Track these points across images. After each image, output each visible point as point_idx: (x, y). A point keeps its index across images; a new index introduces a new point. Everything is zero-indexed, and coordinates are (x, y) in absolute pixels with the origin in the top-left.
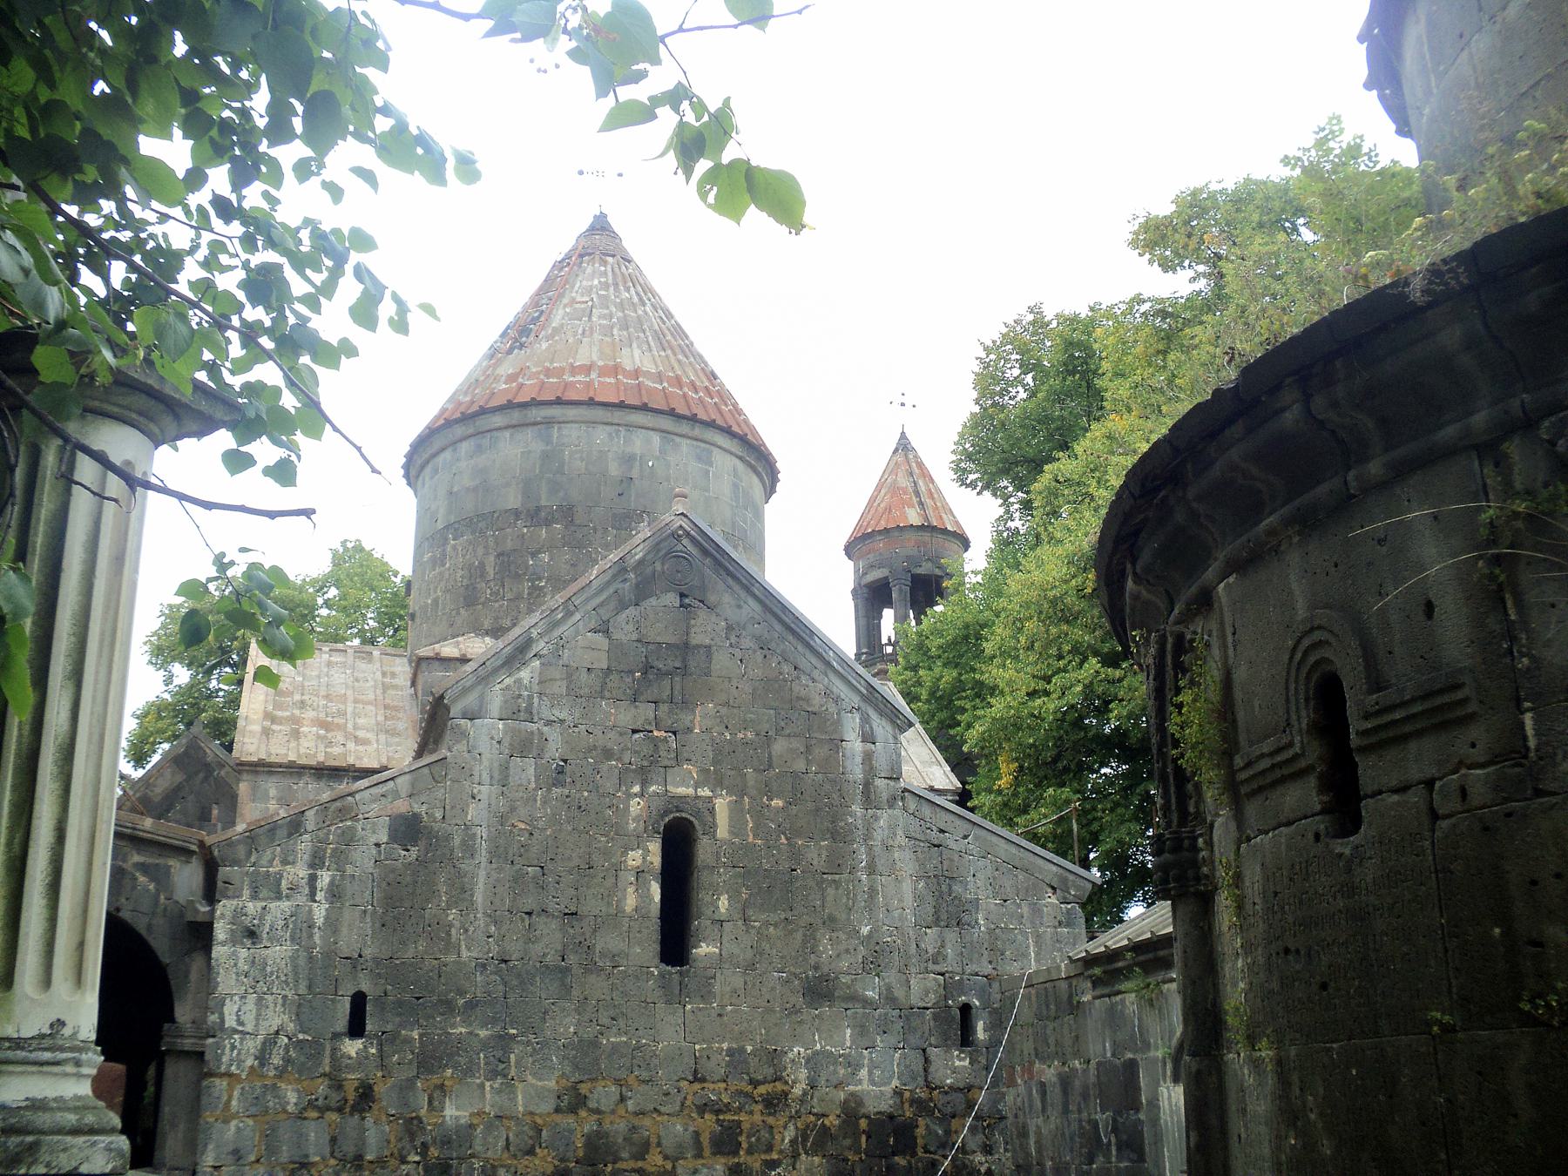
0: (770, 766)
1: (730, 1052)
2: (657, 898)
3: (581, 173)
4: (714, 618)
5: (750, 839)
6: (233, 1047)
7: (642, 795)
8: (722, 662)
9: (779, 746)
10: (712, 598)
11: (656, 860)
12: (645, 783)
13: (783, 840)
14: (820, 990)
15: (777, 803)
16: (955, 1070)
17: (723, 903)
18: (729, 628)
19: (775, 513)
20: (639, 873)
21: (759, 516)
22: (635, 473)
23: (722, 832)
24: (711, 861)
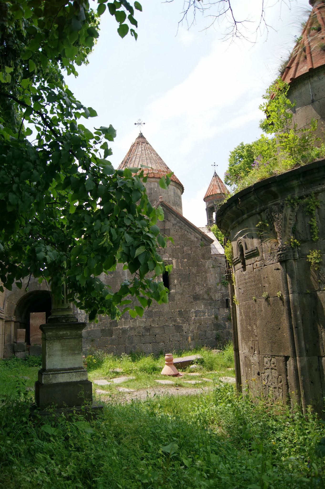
0: (184, 253)
1: (179, 311)
3: (135, 124)
4: (170, 223)
6: (80, 317)
8: (172, 232)
9: (185, 248)
10: (169, 219)
14: (196, 298)
15: (186, 260)
16: (225, 313)
17: (176, 281)
18: (173, 225)
19: (184, 197)
21: (180, 198)
22: (152, 192)
24: (172, 273)
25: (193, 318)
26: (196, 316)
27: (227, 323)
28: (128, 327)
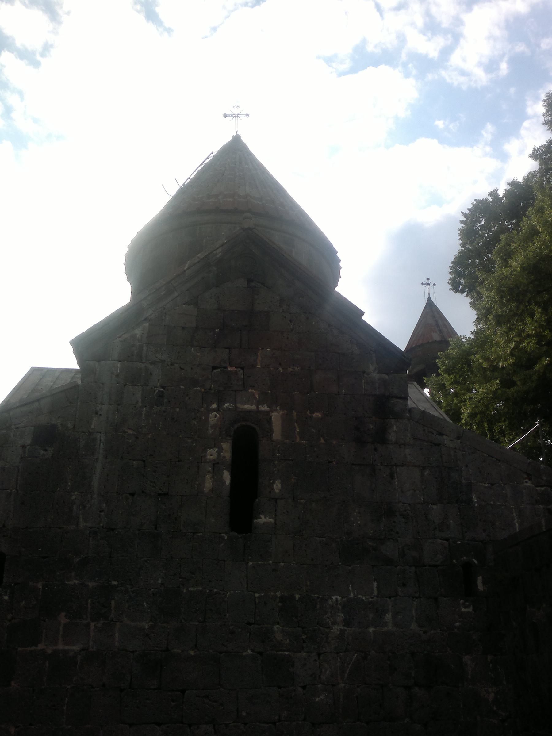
2: (228, 482)
5: (298, 440)
7: (217, 410)
11: (227, 455)
12: (220, 403)
13: (322, 441)
17: (277, 486)
20: (215, 464)
23: (277, 434)
25: (336, 629)
26: (347, 623)
27: (467, 659)
28: (76, 648)
